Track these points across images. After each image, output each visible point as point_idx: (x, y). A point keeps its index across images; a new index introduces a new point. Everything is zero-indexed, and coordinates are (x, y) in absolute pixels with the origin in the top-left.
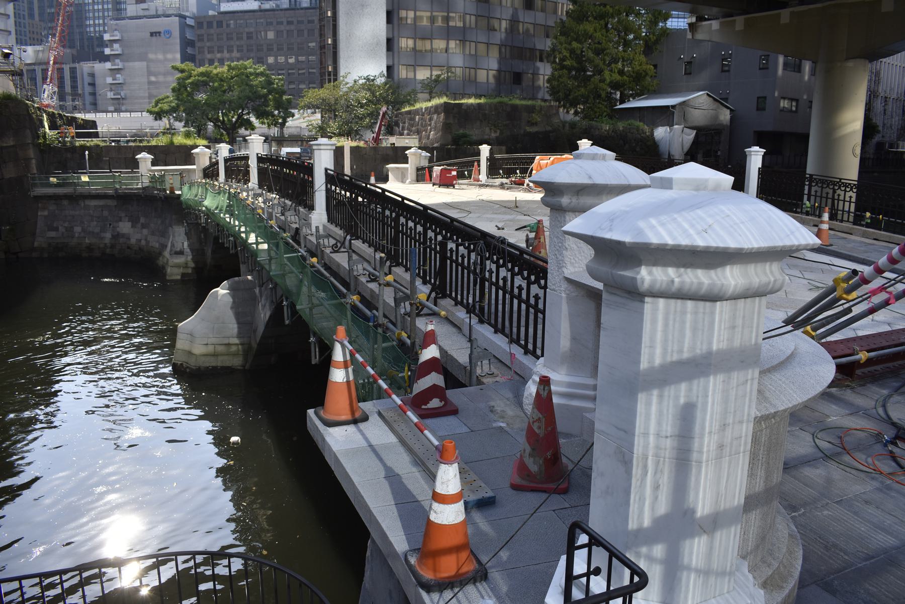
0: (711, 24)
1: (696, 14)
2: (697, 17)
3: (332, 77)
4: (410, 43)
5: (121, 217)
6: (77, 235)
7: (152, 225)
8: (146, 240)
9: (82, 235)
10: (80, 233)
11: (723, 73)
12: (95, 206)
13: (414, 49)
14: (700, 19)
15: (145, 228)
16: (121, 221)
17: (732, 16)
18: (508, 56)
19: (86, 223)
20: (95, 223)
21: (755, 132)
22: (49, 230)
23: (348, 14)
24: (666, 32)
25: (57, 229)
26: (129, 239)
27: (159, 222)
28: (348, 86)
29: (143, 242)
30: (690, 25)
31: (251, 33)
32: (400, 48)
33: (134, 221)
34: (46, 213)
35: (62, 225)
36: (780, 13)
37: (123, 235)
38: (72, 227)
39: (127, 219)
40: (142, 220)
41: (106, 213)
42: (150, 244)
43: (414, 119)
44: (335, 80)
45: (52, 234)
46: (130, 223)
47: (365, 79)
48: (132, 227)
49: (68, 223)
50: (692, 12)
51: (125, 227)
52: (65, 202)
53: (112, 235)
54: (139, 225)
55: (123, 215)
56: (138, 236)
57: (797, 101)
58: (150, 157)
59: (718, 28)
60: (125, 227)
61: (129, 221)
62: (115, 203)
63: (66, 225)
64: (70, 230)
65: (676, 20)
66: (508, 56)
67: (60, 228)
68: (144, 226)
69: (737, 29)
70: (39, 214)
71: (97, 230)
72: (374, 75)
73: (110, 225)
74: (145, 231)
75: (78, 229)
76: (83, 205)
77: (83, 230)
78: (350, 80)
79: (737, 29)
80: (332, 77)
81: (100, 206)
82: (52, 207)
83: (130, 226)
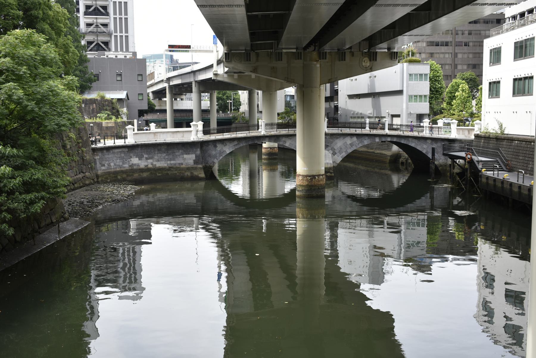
5: (131, 156)
6: (113, 167)
9: (115, 167)
10: (114, 166)
12: (117, 152)
16: (131, 158)
20: (119, 160)
25: (104, 165)
37: (135, 165)
39: (135, 156)
41: (123, 155)
45: (103, 168)
46: (138, 158)
48: (139, 160)
51: (135, 161)
52: (105, 151)
55: (132, 155)
60: (135, 161)
61: (136, 157)
62: (127, 150)
63: (107, 162)
64: (109, 165)
67: (105, 164)
71: (121, 164)
73: (126, 160)
75: (112, 164)
76: (112, 152)
77: (115, 165)
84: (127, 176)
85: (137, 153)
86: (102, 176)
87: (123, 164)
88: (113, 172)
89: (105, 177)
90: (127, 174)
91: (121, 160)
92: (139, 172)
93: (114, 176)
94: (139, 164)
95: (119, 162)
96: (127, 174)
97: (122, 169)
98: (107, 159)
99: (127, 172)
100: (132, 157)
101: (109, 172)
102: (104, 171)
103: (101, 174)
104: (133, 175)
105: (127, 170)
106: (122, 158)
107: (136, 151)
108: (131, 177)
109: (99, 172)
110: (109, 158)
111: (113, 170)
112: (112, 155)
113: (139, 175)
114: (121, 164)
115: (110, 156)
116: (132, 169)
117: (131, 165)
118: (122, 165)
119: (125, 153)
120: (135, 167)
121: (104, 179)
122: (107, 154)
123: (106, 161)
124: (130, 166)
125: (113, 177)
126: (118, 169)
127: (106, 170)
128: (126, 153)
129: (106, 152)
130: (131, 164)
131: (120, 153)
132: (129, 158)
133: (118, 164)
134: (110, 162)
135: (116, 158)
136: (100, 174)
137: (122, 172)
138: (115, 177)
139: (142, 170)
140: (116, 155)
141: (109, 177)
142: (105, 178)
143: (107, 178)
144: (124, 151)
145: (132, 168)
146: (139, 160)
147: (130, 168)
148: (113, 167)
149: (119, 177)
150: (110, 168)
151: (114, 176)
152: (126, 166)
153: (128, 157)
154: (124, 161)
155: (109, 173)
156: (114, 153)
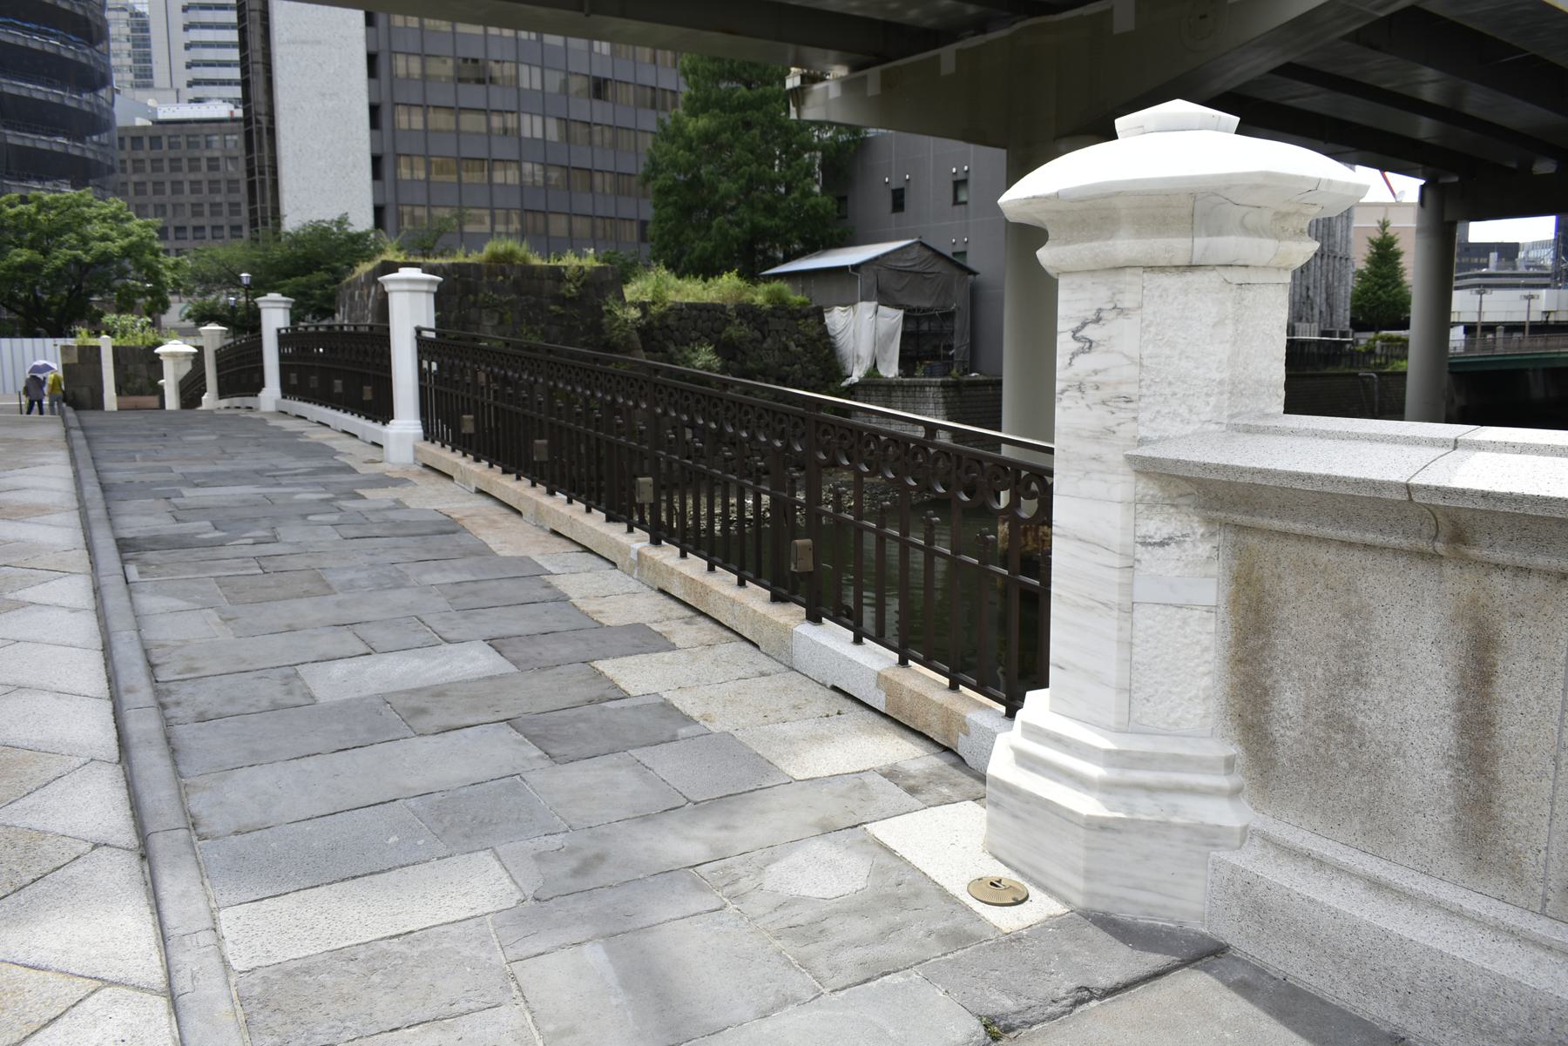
23: (295, 109)
31: (217, 159)
66: (608, 189)
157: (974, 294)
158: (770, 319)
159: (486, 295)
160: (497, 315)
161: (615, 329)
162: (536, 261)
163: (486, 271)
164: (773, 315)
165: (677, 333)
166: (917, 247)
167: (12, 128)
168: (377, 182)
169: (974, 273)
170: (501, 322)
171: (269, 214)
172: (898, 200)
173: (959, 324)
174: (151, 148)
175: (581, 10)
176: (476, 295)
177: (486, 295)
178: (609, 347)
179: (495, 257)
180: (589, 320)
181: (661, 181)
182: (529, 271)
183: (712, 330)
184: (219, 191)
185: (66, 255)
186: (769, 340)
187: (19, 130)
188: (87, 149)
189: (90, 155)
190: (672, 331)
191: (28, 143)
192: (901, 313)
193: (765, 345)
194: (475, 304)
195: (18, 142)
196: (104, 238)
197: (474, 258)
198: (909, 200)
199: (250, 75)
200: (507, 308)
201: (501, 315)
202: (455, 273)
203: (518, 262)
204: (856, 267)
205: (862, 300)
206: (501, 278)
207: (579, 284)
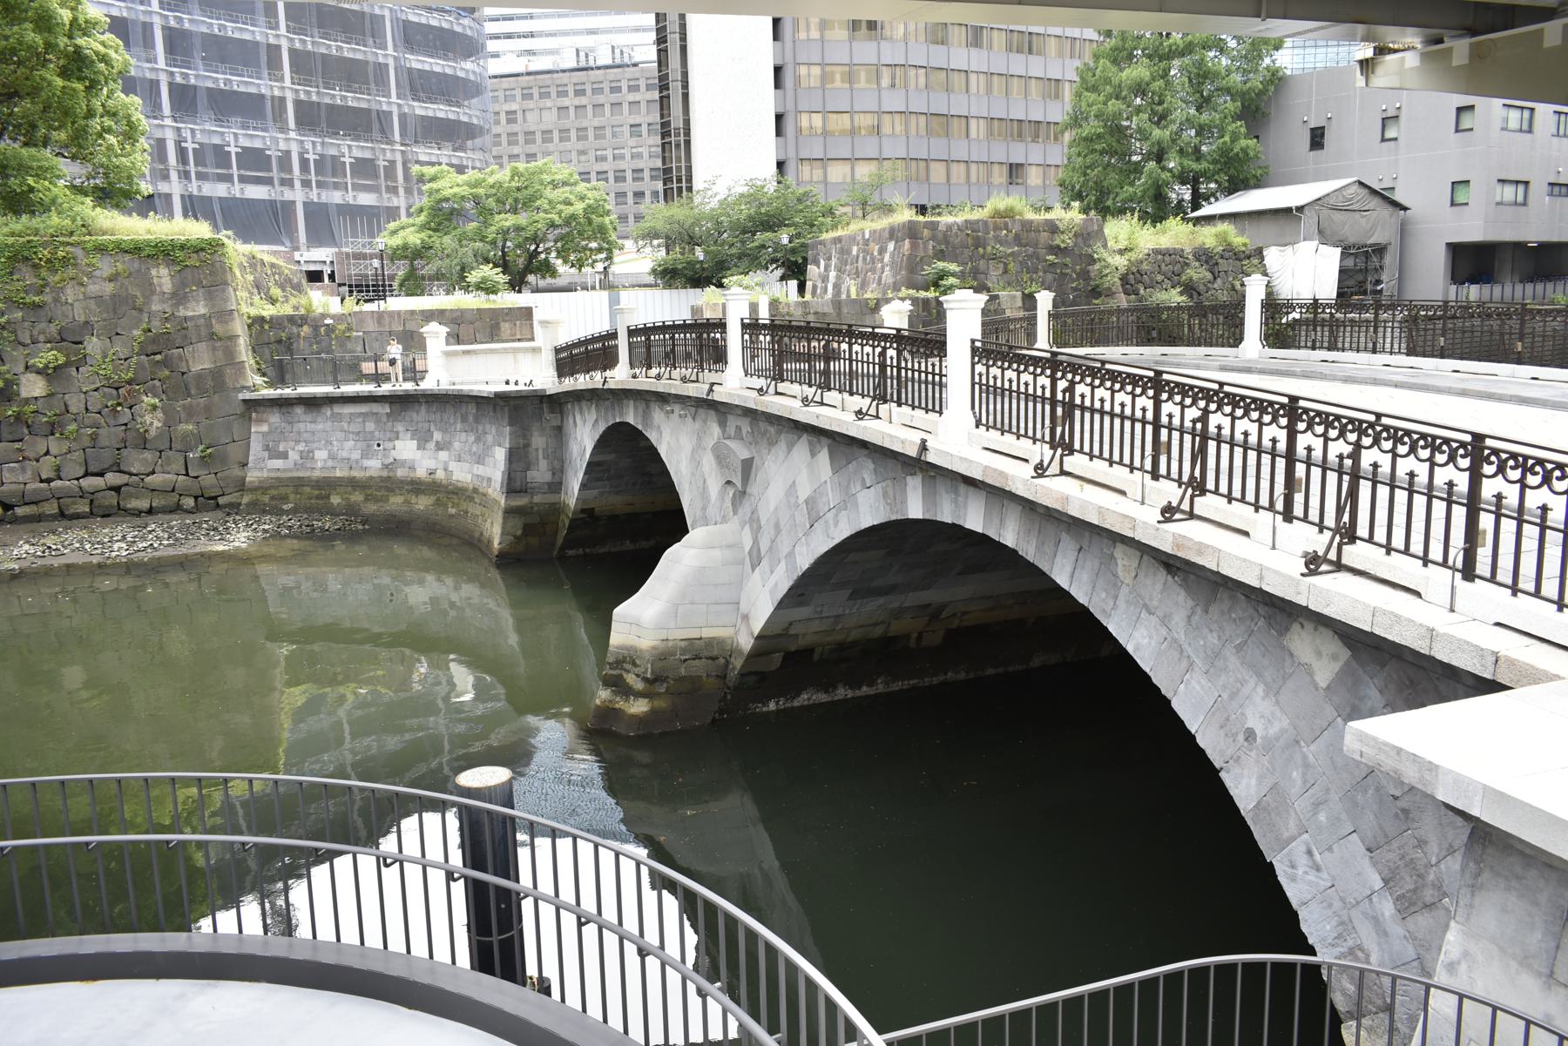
0: (1403, 58)
1: (1374, 42)
2: (1375, 48)
3: (684, 185)
4: (817, 120)
5: (398, 433)
7: (457, 445)
8: (445, 470)
9: (330, 463)
10: (325, 461)
11: (1383, 144)
13: (825, 133)
14: (1381, 51)
15: (442, 449)
16: (398, 439)
17: (1440, 41)
18: (981, 137)
19: (335, 443)
21: (1448, 245)
22: (270, 459)
24: (1277, 79)
25: (284, 456)
26: (412, 468)
27: (472, 438)
28: (718, 198)
29: (440, 475)
30: (1366, 65)
32: (799, 130)
33: (423, 440)
34: (265, 428)
35: (293, 449)
36: (1542, 30)
37: (403, 463)
38: (313, 452)
40: (437, 436)
41: (370, 426)
42: (454, 478)
43: (849, 252)
44: (690, 189)
45: (278, 463)
47: (747, 185)
49: (304, 444)
50: (1366, 39)
52: (299, 410)
53: (383, 464)
54: (431, 445)
55: (400, 427)
56: (431, 464)
57: (1527, 183)
58: (444, 330)
59: (1418, 64)
61: (412, 439)
63: (301, 447)
64: (307, 456)
65: (1301, 51)
66: (981, 137)
67: (290, 453)
68: (440, 447)
69: (1454, 64)
70: (253, 430)
71: (356, 455)
72: (762, 177)
73: (379, 445)
74: (443, 455)
75: (321, 455)
76: (329, 413)
77: (332, 457)
78: (723, 190)
79: (1454, 64)
80: (684, 185)
81: (360, 414)
82: (275, 418)
83: (415, 447)
84: (366, 499)
85: (417, 423)
86: (262, 488)
87: (365, 456)
88: (317, 481)
89: (273, 492)
90: (369, 492)
91: (359, 444)
92: (409, 491)
93: (317, 492)
94: (414, 461)
95: (350, 449)
96: (369, 492)
97: (355, 473)
98: (305, 435)
99: (370, 487)
100: (401, 435)
101: (299, 478)
102: (273, 475)
103: (260, 482)
104: (385, 500)
105: (371, 478)
106: (363, 437)
107: (415, 415)
108: (381, 504)
109: (253, 476)
110: (313, 433)
111: (317, 474)
112: (329, 424)
113: (407, 502)
114: (356, 455)
115: (320, 427)
116: (389, 477)
117: (391, 463)
118: (357, 462)
119: (378, 421)
120: (400, 473)
121: (266, 499)
122: (309, 418)
123: (298, 442)
124: (386, 466)
125: (310, 498)
126: (338, 474)
127: (285, 470)
128: (384, 419)
129: (305, 413)
130: (392, 460)
131: (361, 420)
132: (390, 440)
133: (345, 454)
134: (315, 445)
135: (340, 435)
136: (251, 482)
137: (354, 484)
138: (318, 497)
139: (417, 487)
140: (345, 425)
141: (292, 497)
142: (272, 498)
143: (284, 499)
144: (377, 414)
145: (391, 474)
146: (418, 449)
147: (385, 474)
148: (319, 465)
149: (335, 500)
150: (309, 465)
151: (317, 492)
152: (373, 466)
153: (388, 435)
154: (369, 446)
155: (298, 483)
156: (337, 418)
157: (1404, 230)
158: (1220, 261)
159: (993, 247)
160: (1001, 265)
161: (1106, 275)
162: (1030, 215)
163: (991, 226)
164: (1222, 257)
165: (1132, 276)
166: (1355, 188)
167: (419, 100)
168: (779, 138)
169: (1405, 209)
170: (1006, 271)
171: (684, 173)
172: (1317, 139)
173: (1390, 259)
174: (594, 117)
175: (1259, 17)
176: (984, 248)
177: (993, 247)
178: (1096, 292)
179: (998, 214)
180: (1078, 267)
181: (1086, 131)
182: (1027, 226)
183: (1173, 273)
184: (517, 143)
185: (544, 219)
186: (1219, 280)
187: (424, 102)
188: (465, 114)
189: (475, 121)
190: (1142, 275)
191: (430, 114)
192: (1340, 249)
193: (1216, 286)
194: (983, 257)
195: (423, 113)
196: (568, 203)
197: (977, 215)
198: (1328, 139)
199: (668, 44)
200: (1010, 259)
201: (1006, 265)
202: (967, 228)
203: (1018, 217)
204: (1300, 209)
205: (1305, 240)
206: (1005, 232)
207: (1071, 235)
